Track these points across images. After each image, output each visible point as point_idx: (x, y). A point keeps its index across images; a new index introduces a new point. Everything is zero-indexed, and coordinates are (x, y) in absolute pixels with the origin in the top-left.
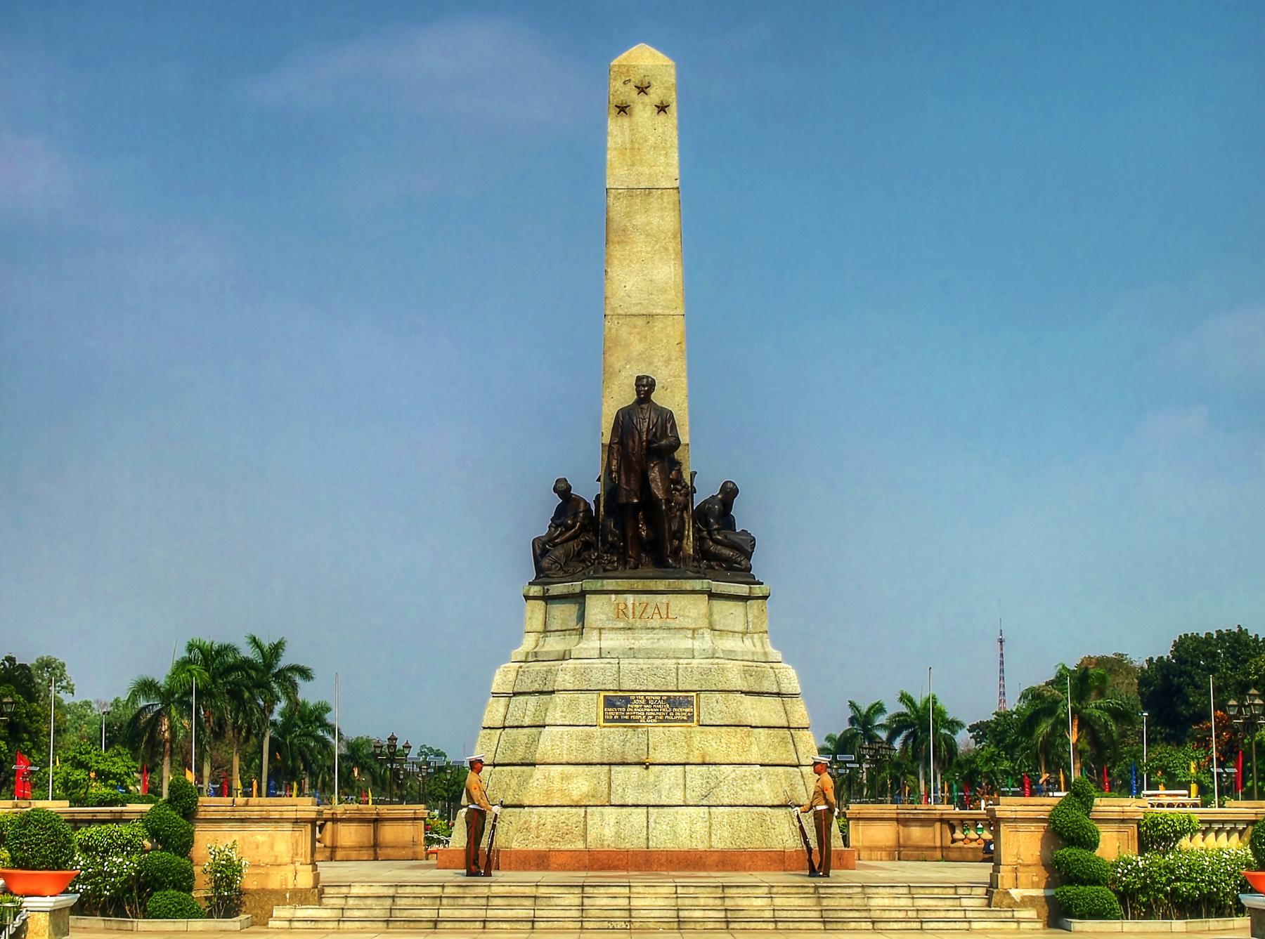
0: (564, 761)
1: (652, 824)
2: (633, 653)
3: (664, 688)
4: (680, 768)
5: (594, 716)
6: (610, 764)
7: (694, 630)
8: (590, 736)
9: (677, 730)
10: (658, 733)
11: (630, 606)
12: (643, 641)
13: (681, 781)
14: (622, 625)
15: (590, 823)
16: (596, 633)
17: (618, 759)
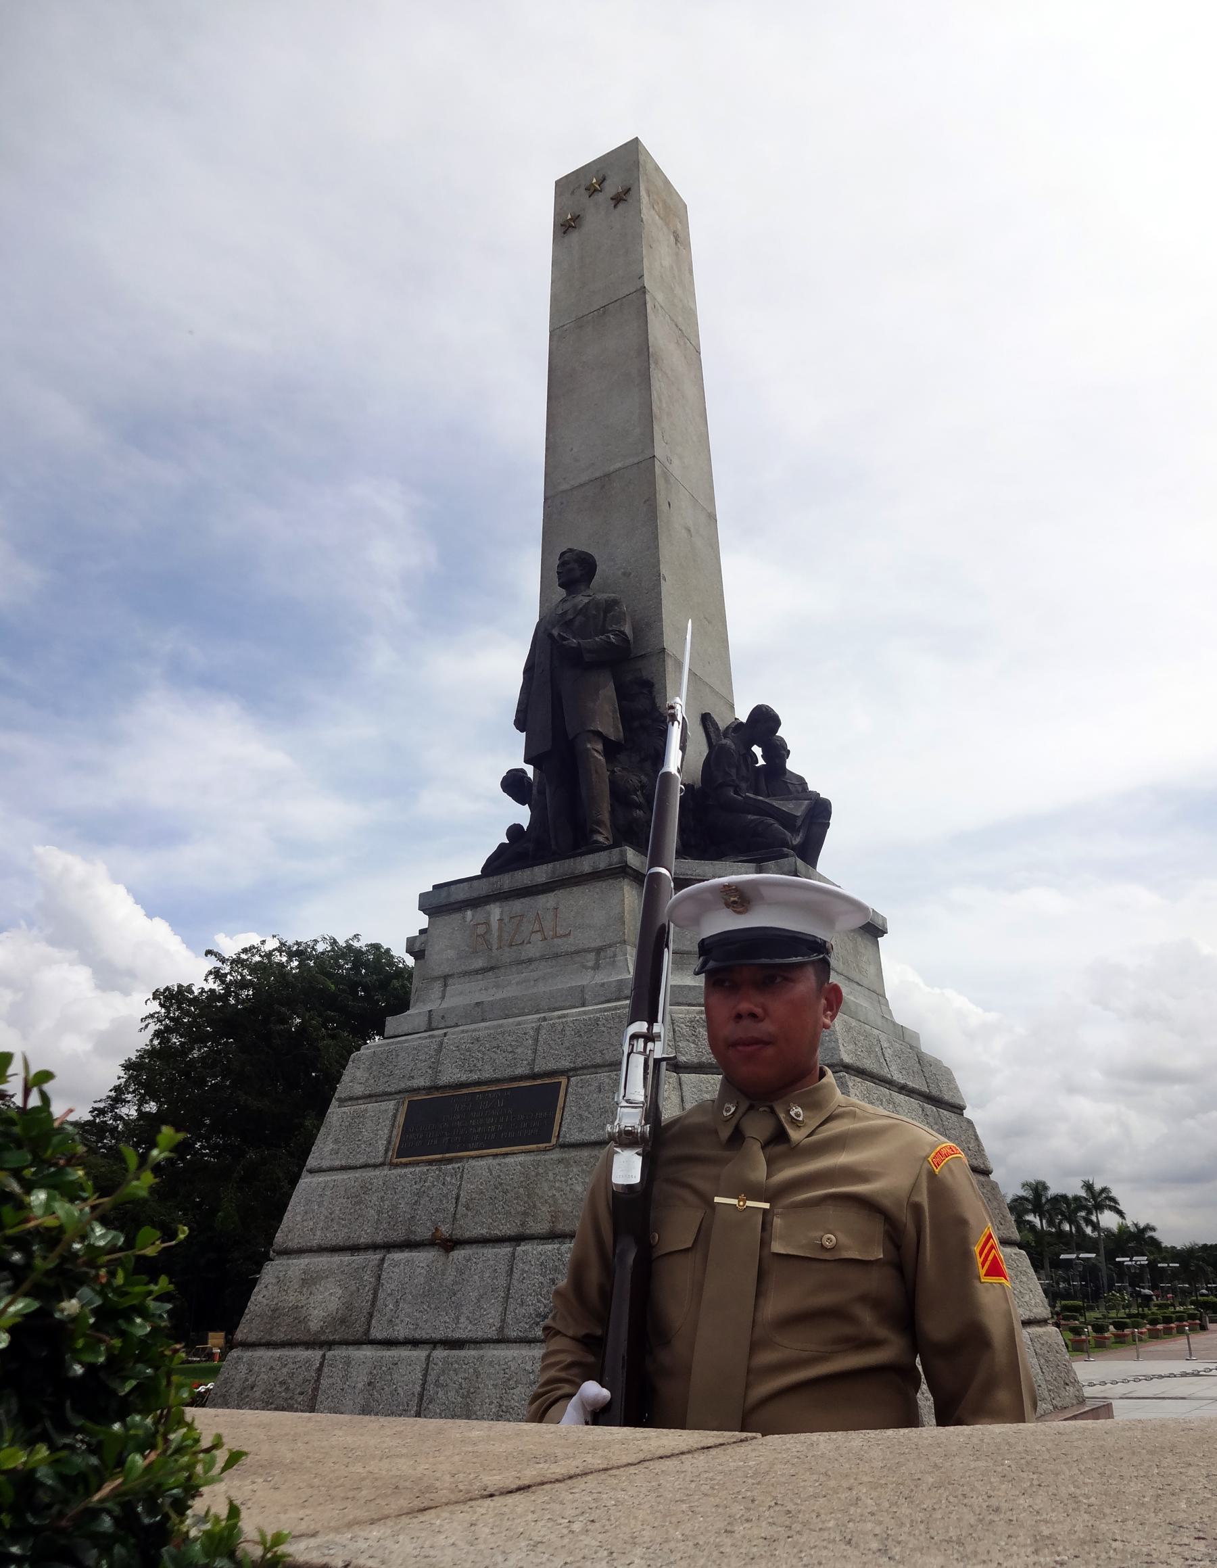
0: (315, 1243)
1: (431, 1388)
2: (479, 1012)
3: (508, 1072)
4: (505, 1250)
5: (381, 1145)
6: (389, 1247)
7: (599, 951)
8: (366, 1188)
9: (515, 1162)
10: (483, 1170)
11: (495, 925)
12: (511, 987)
13: (502, 1281)
14: (479, 963)
15: (324, 1382)
16: (438, 986)
17: (398, 1235)
